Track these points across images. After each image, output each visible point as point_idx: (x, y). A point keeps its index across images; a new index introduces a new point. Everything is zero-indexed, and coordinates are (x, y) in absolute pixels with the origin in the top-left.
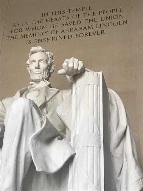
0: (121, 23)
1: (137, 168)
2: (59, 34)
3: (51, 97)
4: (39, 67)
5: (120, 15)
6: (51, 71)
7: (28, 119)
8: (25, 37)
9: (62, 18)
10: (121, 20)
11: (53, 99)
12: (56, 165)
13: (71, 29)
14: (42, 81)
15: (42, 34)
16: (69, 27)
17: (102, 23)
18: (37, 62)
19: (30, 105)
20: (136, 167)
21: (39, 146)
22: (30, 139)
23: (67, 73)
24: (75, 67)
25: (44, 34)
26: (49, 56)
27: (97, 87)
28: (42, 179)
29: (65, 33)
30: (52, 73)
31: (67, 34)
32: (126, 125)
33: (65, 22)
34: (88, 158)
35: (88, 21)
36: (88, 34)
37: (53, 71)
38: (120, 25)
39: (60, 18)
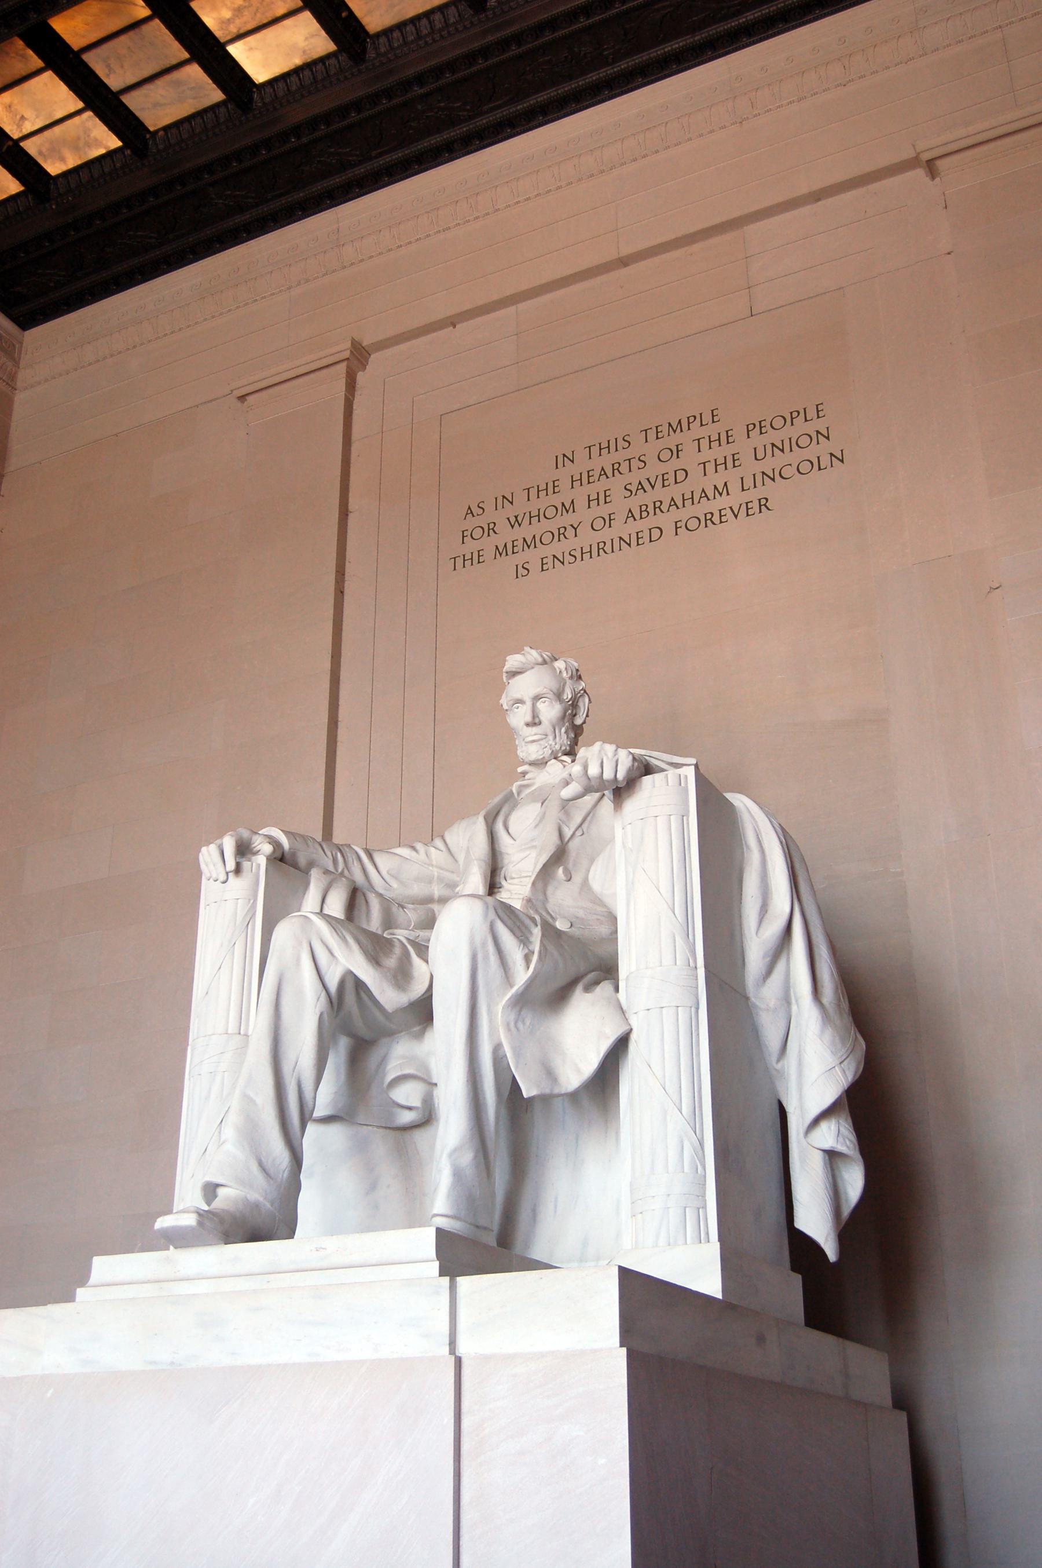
0: (825, 461)
1: (829, 1033)
2: (622, 528)
3: (578, 820)
4: (537, 721)
5: (818, 432)
6: (578, 721)
7: (486, 957)
8: (510, 551)
9: (624, 468)
10: (824, 448)
11: (585, 826)
12: (578, 1071)
13: (658, 504)
14: (553, 761)
15: (561, 534)
16: (648, 498)
17: (759, 467)
18: (529, 704)
19: (486, 915)
20: (822, 1031)
21: (528, 1023)
22: (500, 1008)
23: (588, 790)
24: (608, 775)
25: (570, 532)
26: (564, 674)
27: (680, 821)
28: (558, 1104)
29: (639, 522)
30: (584, 722)
31: (643, 525)
32: (788, 910)
33: (634, 478)
34: (662, 1040)
35: (710, 467)
36: (716, 519)
37: (587, 716)
38: (820, 469)
39: (616, 468)
